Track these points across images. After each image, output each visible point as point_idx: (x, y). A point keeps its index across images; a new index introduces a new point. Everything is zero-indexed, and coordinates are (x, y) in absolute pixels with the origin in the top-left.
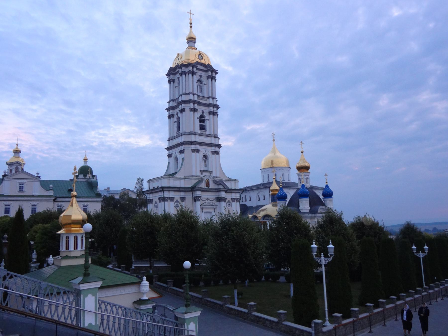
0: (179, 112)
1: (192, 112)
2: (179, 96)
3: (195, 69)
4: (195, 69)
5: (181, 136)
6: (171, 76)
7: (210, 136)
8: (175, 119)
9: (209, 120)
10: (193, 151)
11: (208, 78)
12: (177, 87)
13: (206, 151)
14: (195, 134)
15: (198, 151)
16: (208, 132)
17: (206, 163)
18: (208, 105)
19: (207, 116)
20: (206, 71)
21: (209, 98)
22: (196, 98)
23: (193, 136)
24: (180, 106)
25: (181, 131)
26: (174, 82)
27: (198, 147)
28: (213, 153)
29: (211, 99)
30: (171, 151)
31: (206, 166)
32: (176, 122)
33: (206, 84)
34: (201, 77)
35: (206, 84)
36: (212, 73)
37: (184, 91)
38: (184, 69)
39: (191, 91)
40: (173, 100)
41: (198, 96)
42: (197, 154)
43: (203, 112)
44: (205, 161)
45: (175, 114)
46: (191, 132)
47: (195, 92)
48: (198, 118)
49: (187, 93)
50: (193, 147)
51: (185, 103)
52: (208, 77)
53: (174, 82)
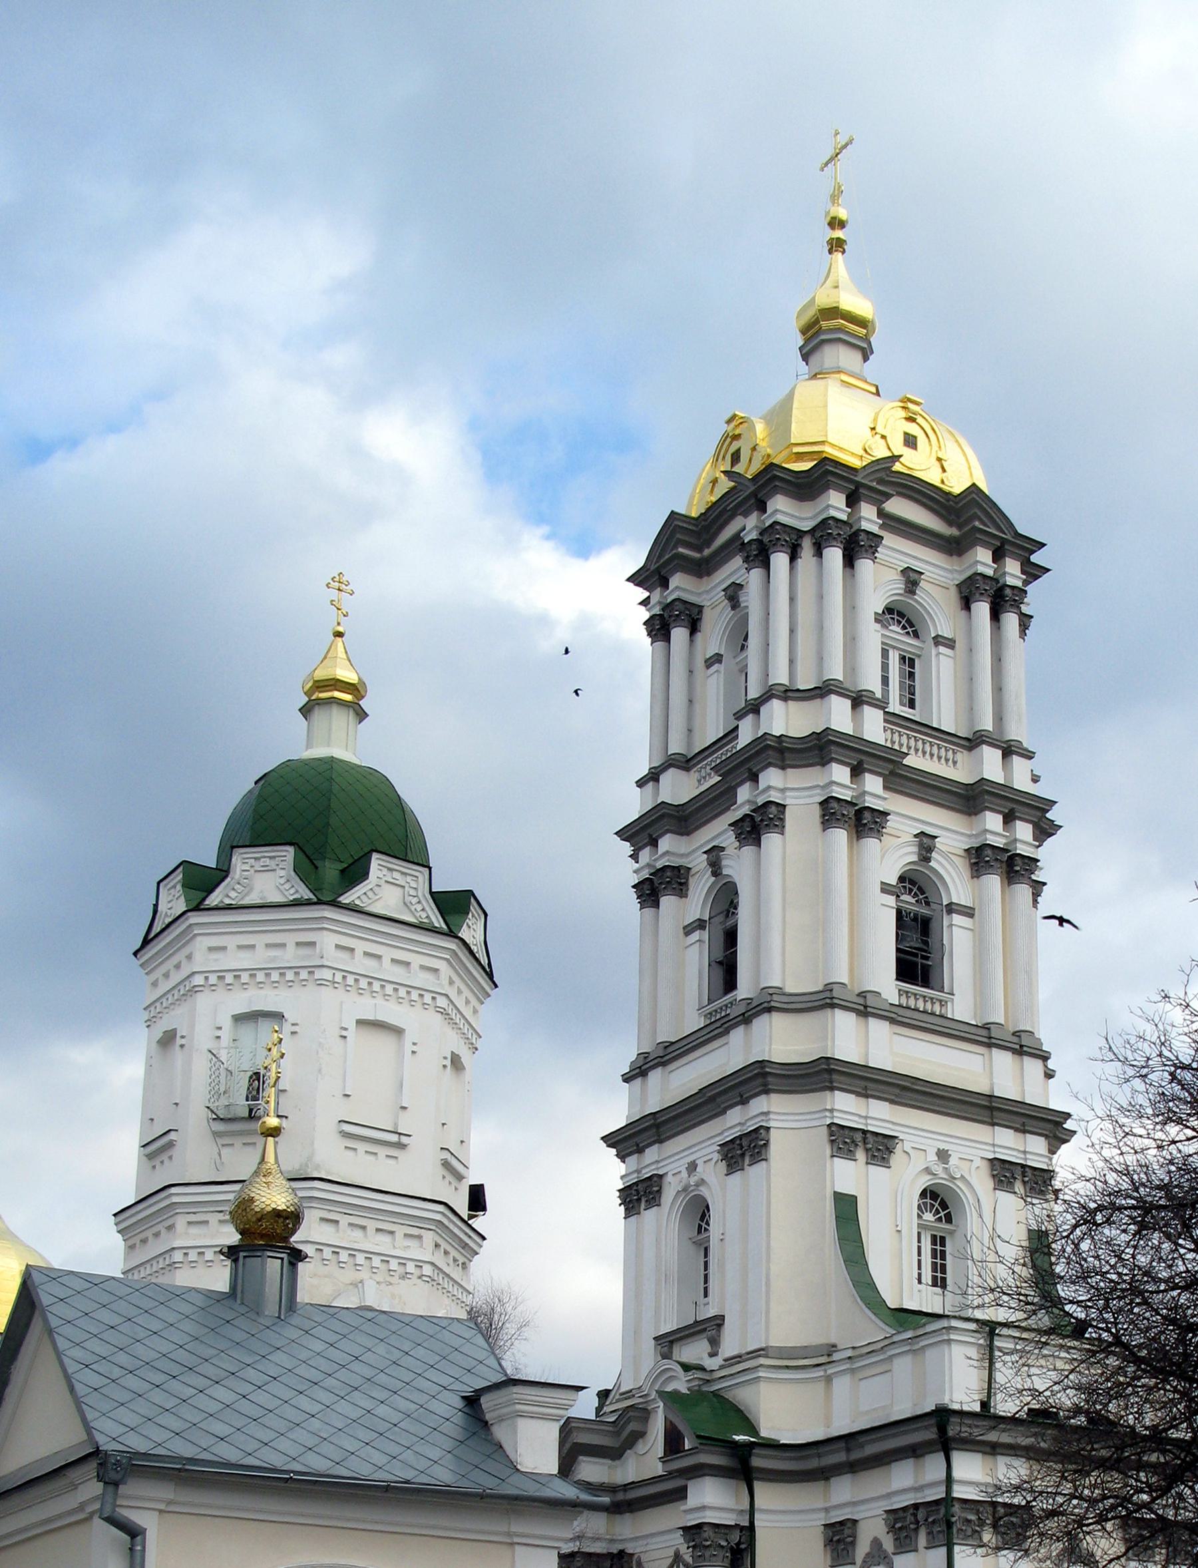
0: (729, 839)
1: (840, 836)
2: (739, 716)
5: (746, 1019)
6: (676, 580)
7: (985, 1037)
8: (697, 901)
9: (969, 912)
10: (844, 1140)
11: (966, 604)
12: (718, 658)
13: (943, 1155)
14: (865, 1007)
15: (880, 1148)
16: (961, 1009)
17: (939, 1254)
18: (971, 799)
19: (956, 883)
20: (954, 547)
21: (973, 742)
22: (873, 728)
23: (844, 1021)
24: (744, 793)
25: (745, 988)
26: (694, 627)
27: (878, 1115)
28: (1005, 1173)
29: (990, 758)
30: (652, 1154)
31: (940, 1282)
32: (700, 924)
33: (950, 644)
34: (911, 580)
35: (950, 644)
36: (998, 556)
37: (780, 676)
38: (784, 509)
39: (836, 671)
40: (685, 763)
41: (892, 719)
42: (876, 1171)
43: (926, 844)
44: (939, 1241)
45: (699, 862)
46: (829, 987)
47: (872, 683)
48: (886, 888)
49: (805, 682)
50: (847, 1107)
52: (967, 594)
53: (694, 627)
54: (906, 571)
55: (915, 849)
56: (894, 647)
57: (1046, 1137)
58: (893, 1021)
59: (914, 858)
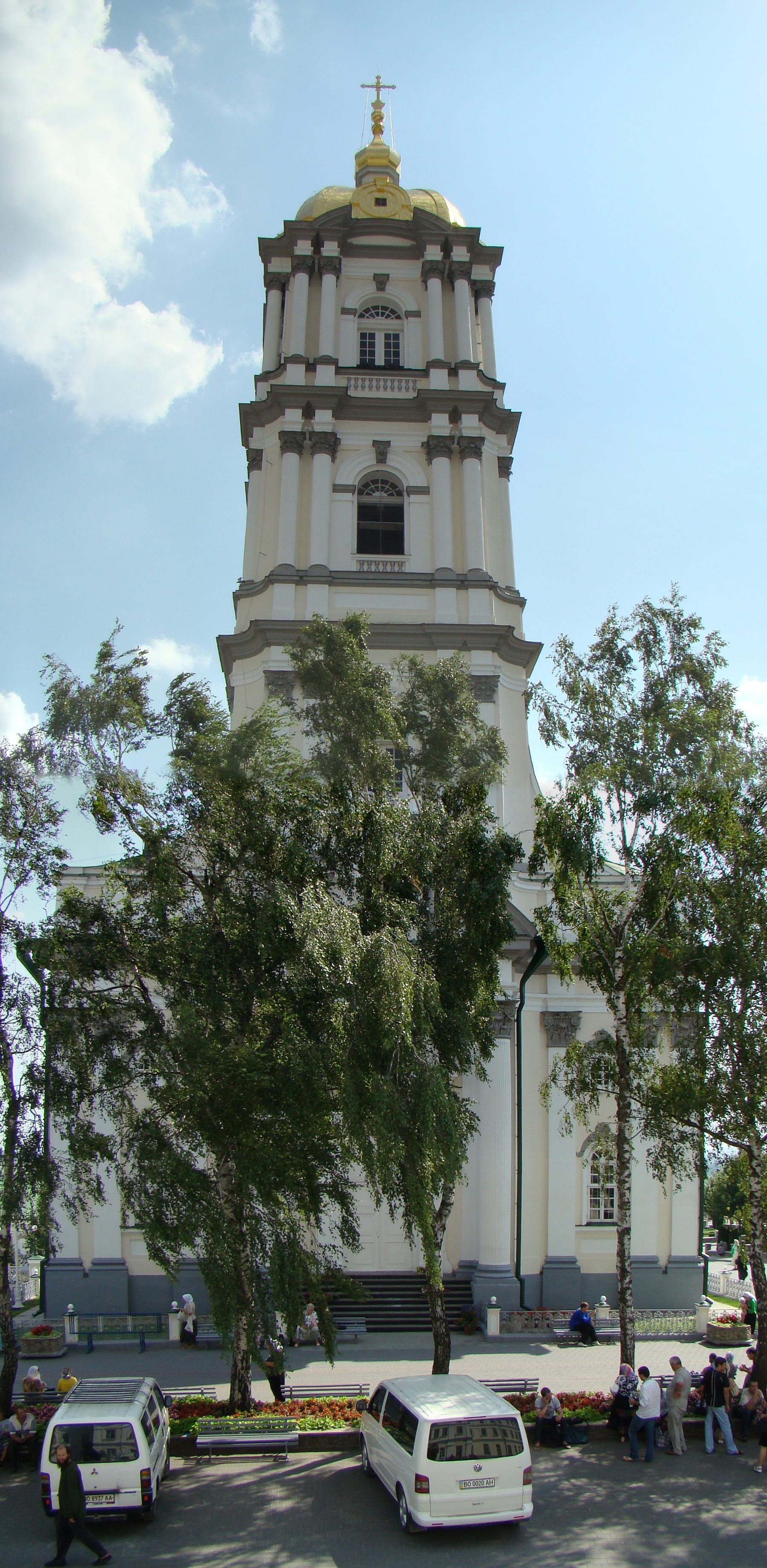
1: (292, 458)
3: (330, 249)
4: (330, 249)
7: (430, 581)
9: (424, 491)
33: (417, 314)
34: (381, 281)
35: (417, 314)
43: (382, 449)
48: (337, 488)
51: (263, 426)
54: (376, 276)
55: (374, 455)
56: (380, 330)
57: (494, 650)
58: (331, 584)
59: (374, 462)
